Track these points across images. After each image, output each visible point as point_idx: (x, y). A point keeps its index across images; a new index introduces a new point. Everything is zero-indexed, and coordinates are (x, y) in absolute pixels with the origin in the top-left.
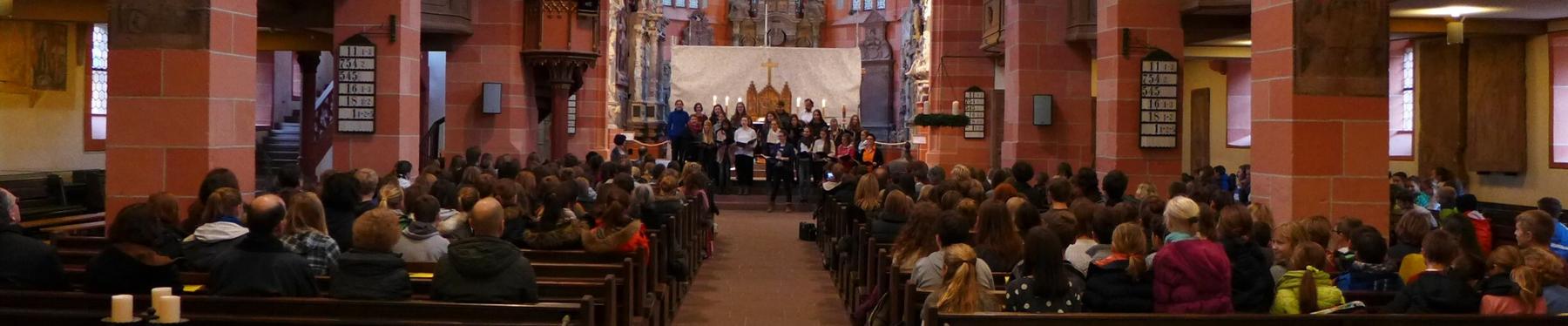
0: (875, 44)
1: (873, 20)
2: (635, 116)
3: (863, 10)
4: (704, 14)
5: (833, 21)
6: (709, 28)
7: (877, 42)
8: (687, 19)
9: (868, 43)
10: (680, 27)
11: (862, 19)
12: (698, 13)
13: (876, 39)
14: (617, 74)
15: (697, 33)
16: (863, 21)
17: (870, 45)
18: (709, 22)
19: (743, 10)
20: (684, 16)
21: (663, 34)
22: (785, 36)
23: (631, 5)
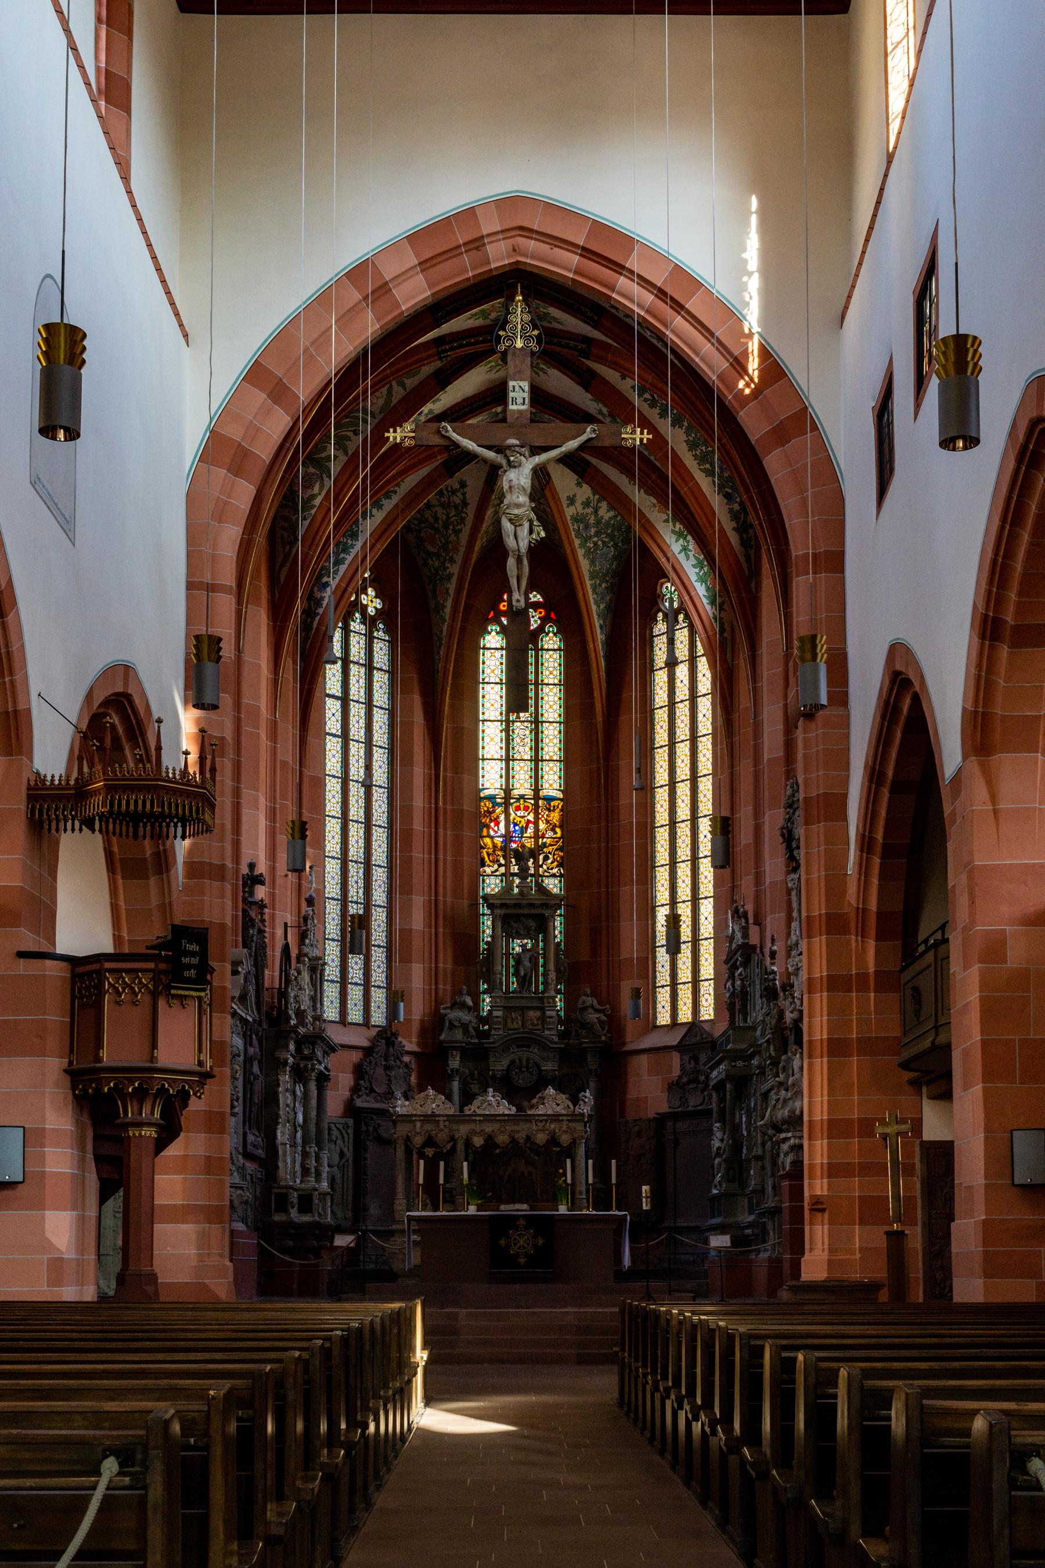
0: (697, 1081)
1: (694, 1040)
2: (276, 1211)
3: (674, 1024)
4: (395, 1035)
5: (624, 1044)
6: (406, 1059)
7: (702, 1078)
8: (365, 1043)
9: (685, 1080)
10: (356, 1056)
11: (674, 1039)
12: (387, 1036)
13: (698, 1072)
14: (245, 1135)
15: (387, 1068)
16: (675, 1043)
17: (689, 1082)
18: (406, 1048)
19: (465, 1026)
20: (360, 1039)
21: (326, 1068)
22: (540, 1071)
23: (268, 1015)
